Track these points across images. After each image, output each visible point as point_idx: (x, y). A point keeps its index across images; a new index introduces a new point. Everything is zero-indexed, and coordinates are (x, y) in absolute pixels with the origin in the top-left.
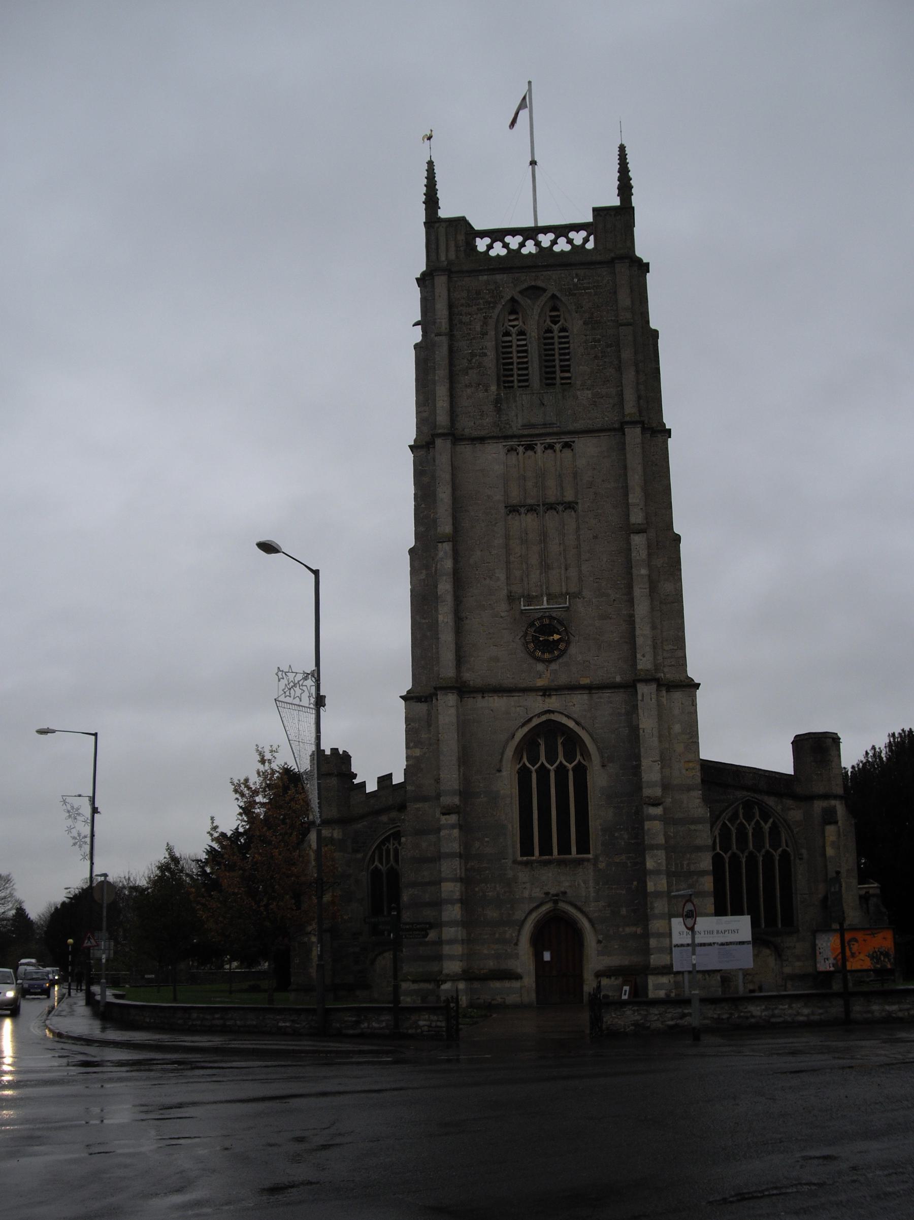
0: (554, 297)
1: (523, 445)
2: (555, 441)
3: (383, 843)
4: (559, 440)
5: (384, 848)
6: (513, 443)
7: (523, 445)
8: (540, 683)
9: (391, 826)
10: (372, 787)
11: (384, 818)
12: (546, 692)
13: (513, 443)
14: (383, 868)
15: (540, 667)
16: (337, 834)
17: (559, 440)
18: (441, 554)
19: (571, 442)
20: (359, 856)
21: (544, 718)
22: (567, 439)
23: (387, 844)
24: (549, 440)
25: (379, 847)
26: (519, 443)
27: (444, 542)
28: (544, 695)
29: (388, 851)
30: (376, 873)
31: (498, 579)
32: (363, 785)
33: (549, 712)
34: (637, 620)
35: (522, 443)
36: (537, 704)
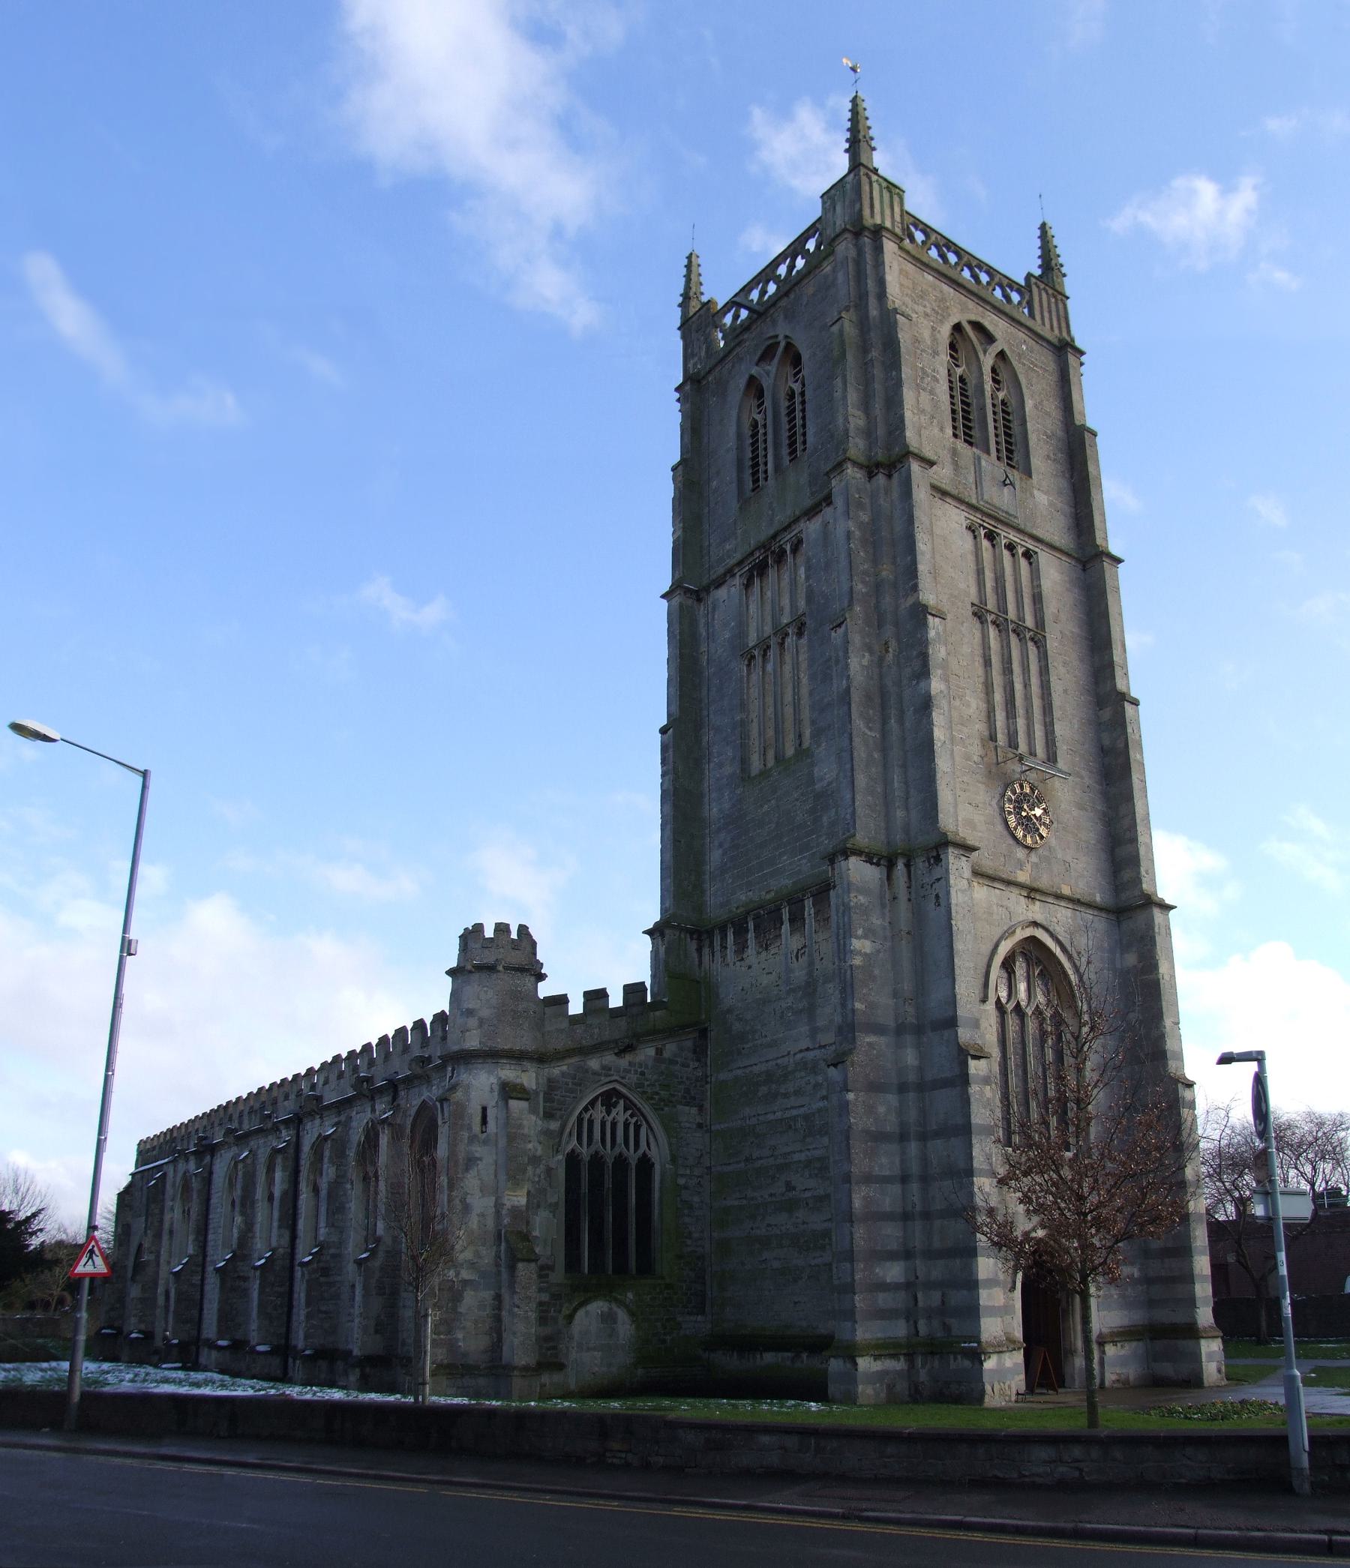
0: (1002, 355)
1: (985, 528)
2: (1018, 541)
3: (586, 1109)
4: (1022, 543)
5: (587, 1116)
6: (975, 519)
7: (985, 528)
8: (1022, 877)
9: (604, 1080)
10: (576, 1007)
11: (594, 1063)
12: (1032, 892)
13: (975, 519)
14: (585, 1152)
15: (1021, 853)
16: (528, 1077)
17: (1022, 543)
18: (932, 634)
19: (1033, 551)
20: (554, 1125)
21: (1029, 932)
22: (1030, 545)
23: (592, 1111)
24: (1014, 537)
25: (580, 1119)
26: (982, 523)
27: (937, 616)
28: (1028, 897)
29: (591, 1122)
30: (572, 1160)
31: (969, 706)
32: (562, 1001)
33: (1035, 924)
34: (1138, 821)
35: (985, 524)
36: (1024, 910)
